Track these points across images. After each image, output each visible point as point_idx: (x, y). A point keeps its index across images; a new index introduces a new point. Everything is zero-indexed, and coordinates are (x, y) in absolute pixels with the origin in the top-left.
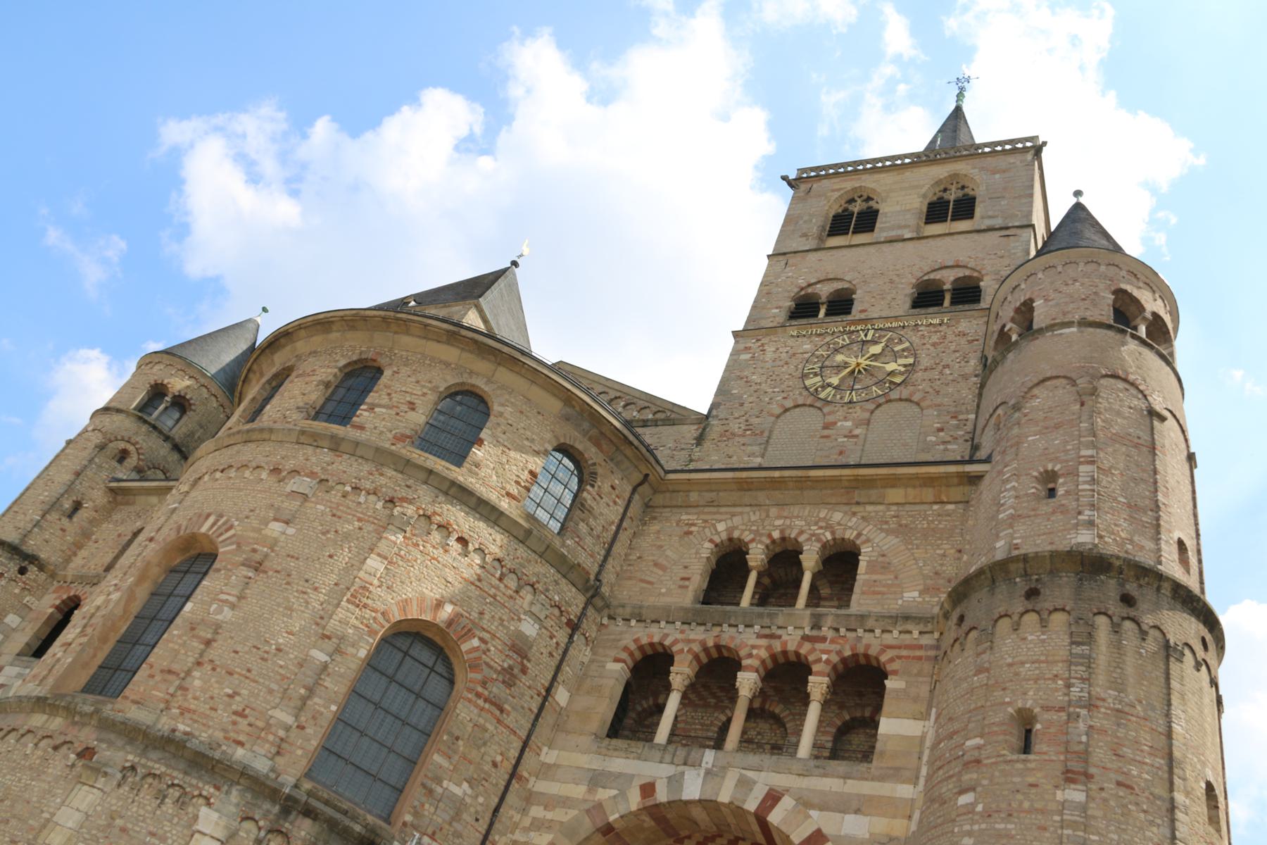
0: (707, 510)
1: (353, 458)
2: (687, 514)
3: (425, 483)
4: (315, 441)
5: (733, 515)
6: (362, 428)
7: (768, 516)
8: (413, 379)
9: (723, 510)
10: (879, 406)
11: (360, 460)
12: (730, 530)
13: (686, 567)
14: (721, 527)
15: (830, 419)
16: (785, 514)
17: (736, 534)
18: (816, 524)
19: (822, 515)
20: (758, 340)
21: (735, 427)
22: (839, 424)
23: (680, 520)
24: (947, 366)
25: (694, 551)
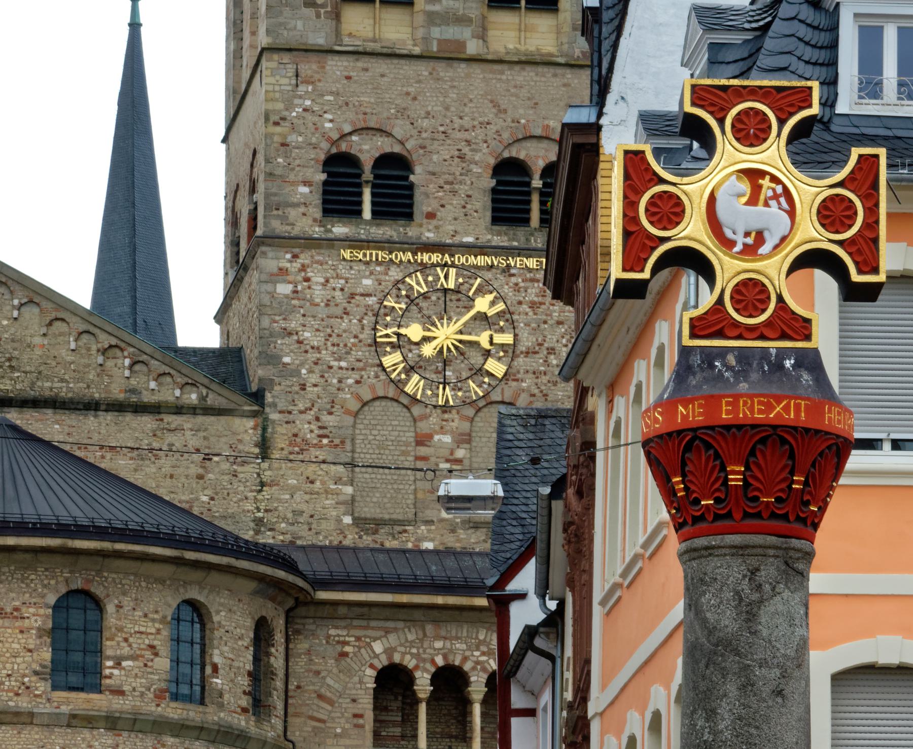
0: (356, 623)
1: (133, 735)
2: (337, 628)
3: (198, 739)
4: (90, 723)
5: (387, 631)
6: (121, 693)
7: (425, 635)
8: (138, 613)
9: (373, 624)
10: (479, 410)
11: (140, 735)
12: (389, 651)
13: (354, 701)
14: (378, 647)
15: (423, 427)
16: (443, 633)
17: (397, 658)
18: (478, 649)
19: (481, 637)
20: (295, 256)
21: (306, 428)
22: (436, 438)
23: (328, 637)
24: (551, 351)
25: (356, 679)
